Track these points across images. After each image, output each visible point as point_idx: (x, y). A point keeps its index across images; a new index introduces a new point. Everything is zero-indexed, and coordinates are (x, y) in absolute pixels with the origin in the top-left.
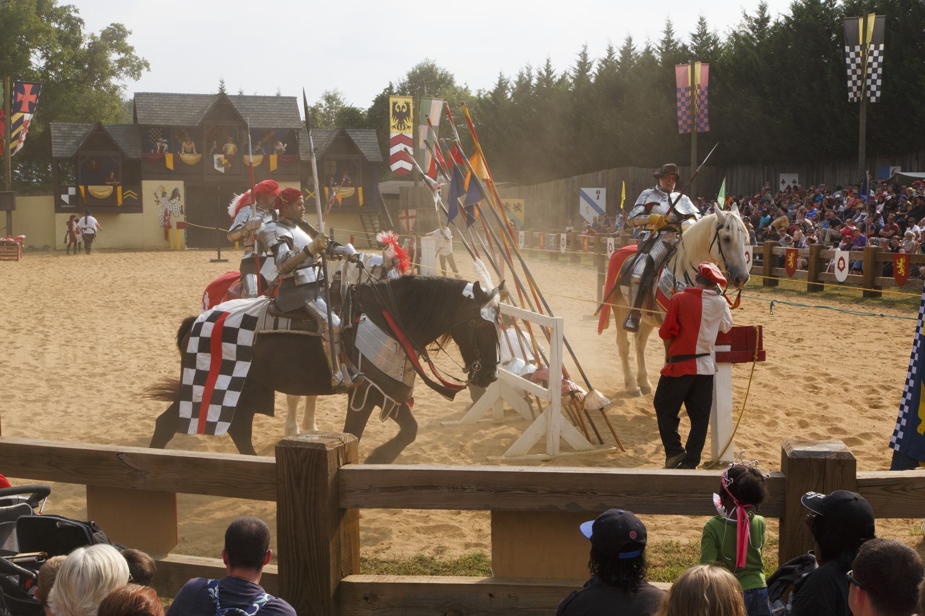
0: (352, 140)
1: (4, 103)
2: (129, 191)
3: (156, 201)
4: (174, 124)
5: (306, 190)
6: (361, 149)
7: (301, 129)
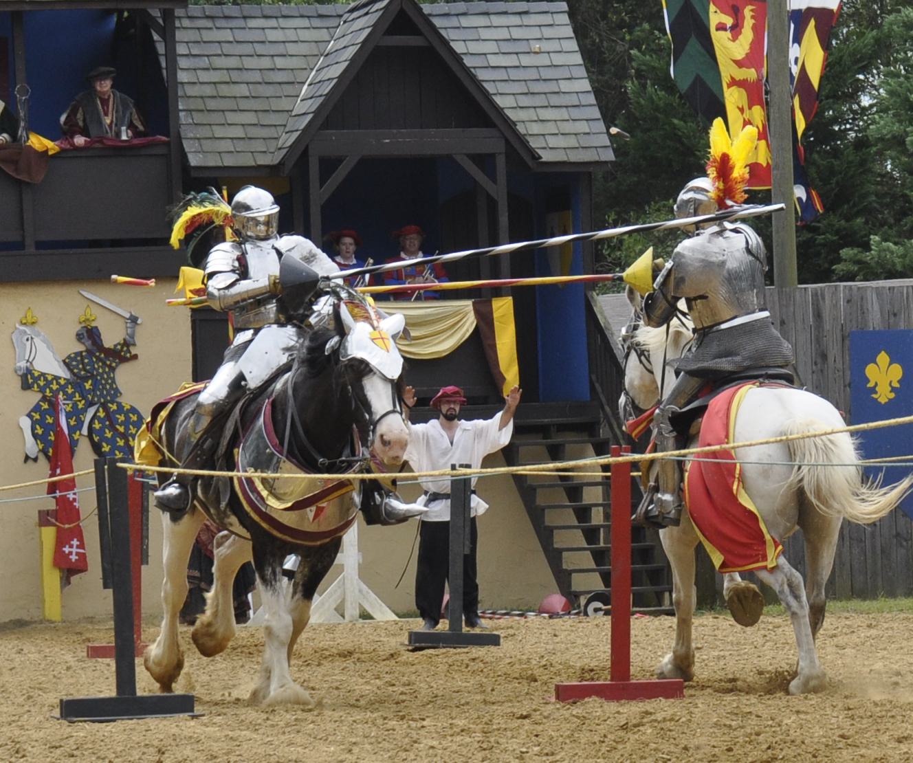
0: (457, 58)
6: (499, 101)
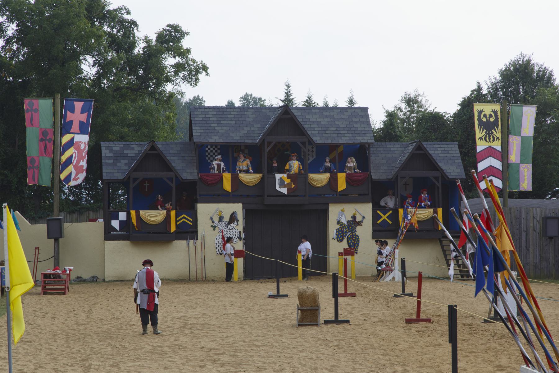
1: (54, 122)
2: (184, 215)
3: (212, 226)
4: (232, 141)
5: (378, 212)
7: (372, 143)
